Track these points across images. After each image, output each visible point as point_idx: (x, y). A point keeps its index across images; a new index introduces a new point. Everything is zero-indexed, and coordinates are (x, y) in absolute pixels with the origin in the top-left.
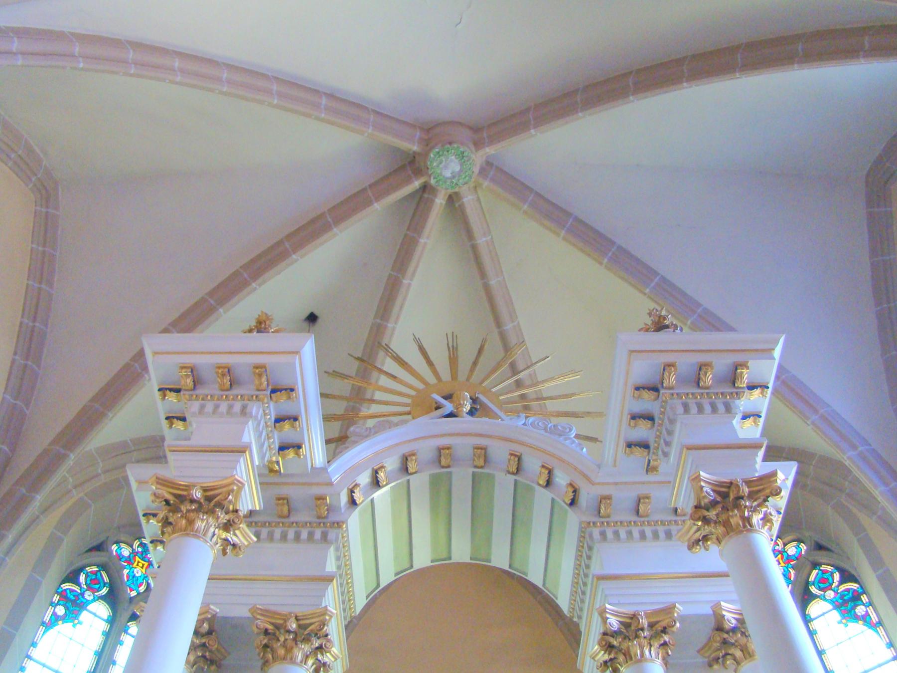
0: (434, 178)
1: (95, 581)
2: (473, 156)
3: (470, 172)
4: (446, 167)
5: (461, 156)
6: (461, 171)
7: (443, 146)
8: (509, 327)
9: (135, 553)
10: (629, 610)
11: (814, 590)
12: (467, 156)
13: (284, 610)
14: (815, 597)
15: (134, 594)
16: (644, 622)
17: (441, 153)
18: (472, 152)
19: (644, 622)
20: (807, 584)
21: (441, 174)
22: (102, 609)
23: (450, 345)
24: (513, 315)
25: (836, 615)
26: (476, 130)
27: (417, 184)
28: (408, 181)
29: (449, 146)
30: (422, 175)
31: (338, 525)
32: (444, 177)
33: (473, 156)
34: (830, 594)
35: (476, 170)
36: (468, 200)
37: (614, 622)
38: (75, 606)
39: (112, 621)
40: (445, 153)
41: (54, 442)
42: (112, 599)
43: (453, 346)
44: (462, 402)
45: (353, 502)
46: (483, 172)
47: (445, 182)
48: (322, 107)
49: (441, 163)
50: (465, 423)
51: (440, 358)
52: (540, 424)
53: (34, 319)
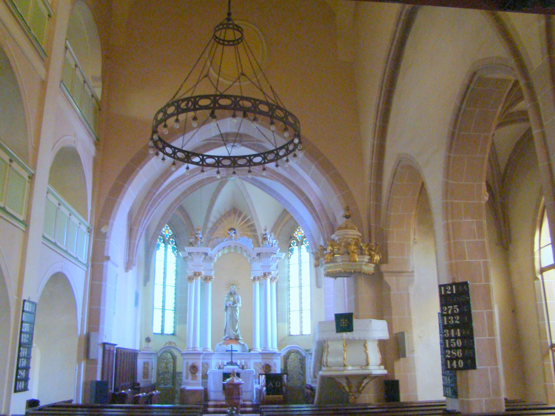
1: (160, 240)
9: (165, 229)
10: (254, 276)
11: (304, 243)
13: (207, 275)
14: (303, 244)
15: (167, 239)
16: (256, 278)
19: (256, 278)
20: (303, 241)
22: (162, 245)
25: (305, 250)
31: (213, 259)
34: (306, 245)
37: (252, 278)
38: (159, 245)
39: (165, 246)
42: (164, 242)
45: (215, 256)
50: (234, 241)
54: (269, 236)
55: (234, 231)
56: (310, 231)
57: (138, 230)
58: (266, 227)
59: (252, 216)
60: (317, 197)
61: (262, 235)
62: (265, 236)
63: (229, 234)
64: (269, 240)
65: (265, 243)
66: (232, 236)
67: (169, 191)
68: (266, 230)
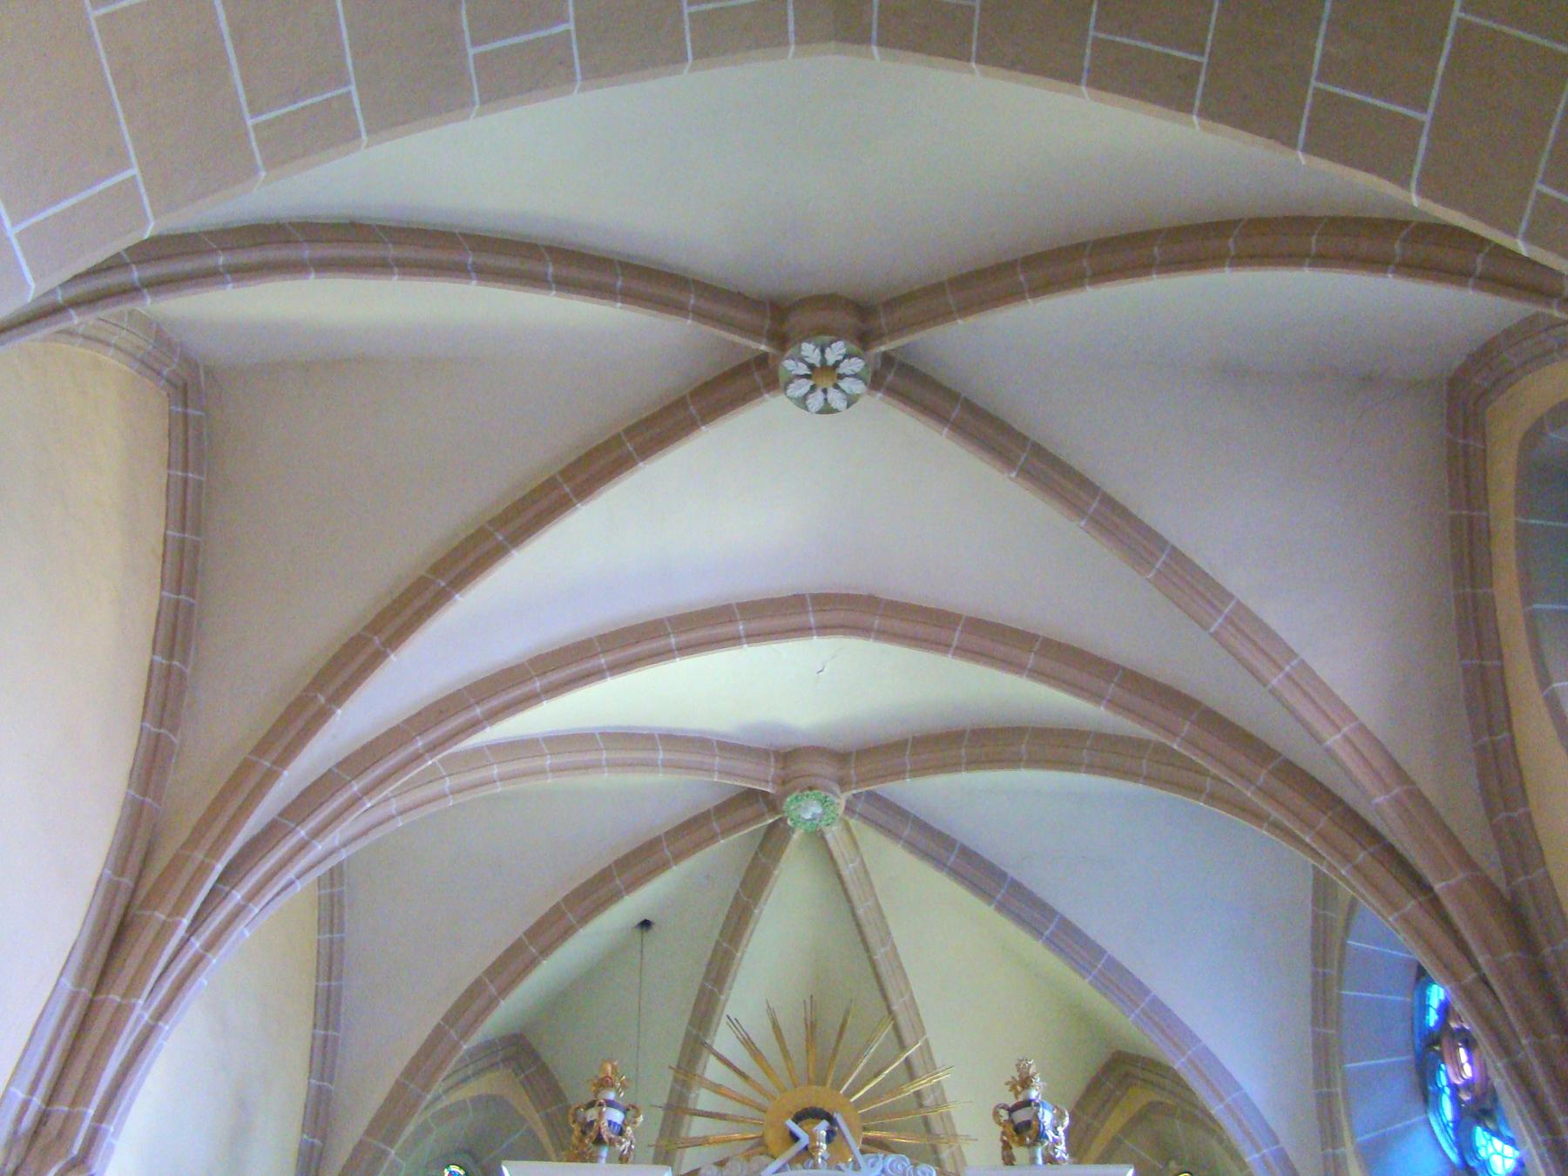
0: (792, 820)
2: (837, 801)
3: (833, 815)
4: (806, 809)
5: (823, 802)
6: (824, 813)
7: (801, 791)
8: (880, 954)
12: (831, 801)
17: (799, 798)
18: (839, 797)
21: (799, 816)
23: (809, 1018)
24: (887, 937)
26: (841, 757)
27: (770, 821)
28: (759, 817)
29: (808, 792)
30: (777, 814)
32: (803, 818)
33: (837, 801)
35: (841, 810)
36: (834, 834)
40: (805, 798)
41: (368, 1132)
43: (812, 1022)
44: (817, 1144)
46: (849, 809)
47: (805, 823)
48: (659, 762)
49: (799, 806)
51: (795, 1037)
52: (899, 1167)
53: (329, 979)
54: (1047, 1117)
55: (822, 1128)
56: (1277, 1142)
57: (166, 930)
58: (1021, 1067)
59: (927, 1042)
60: (1362, 728)
61: (1004, 1114)
62: (1021, 1116)
63: (795, 1138)
64: (1050, 1134)
65: (1019, 1152)
66: (808, 1152)
67: (420, 743)
68: (1026, 1082)
